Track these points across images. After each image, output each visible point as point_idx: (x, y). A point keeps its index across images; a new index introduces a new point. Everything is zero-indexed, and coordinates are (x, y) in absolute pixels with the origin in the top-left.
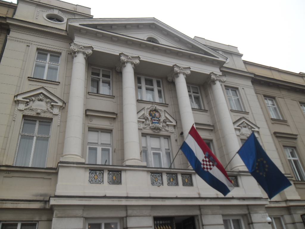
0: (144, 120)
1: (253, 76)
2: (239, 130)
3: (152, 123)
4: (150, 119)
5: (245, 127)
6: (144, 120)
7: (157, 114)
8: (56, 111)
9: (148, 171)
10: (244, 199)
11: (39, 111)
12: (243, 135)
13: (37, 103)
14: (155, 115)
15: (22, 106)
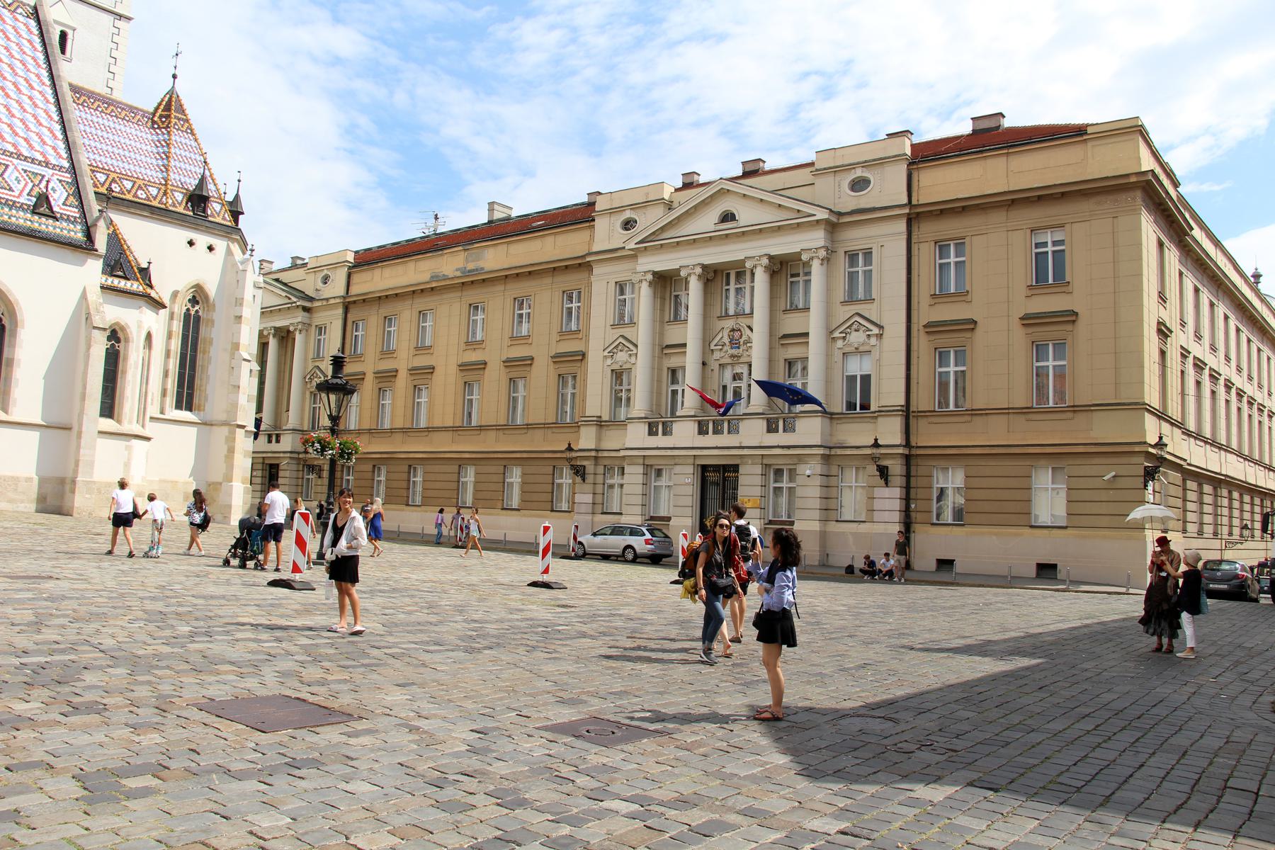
0: (720, 347)
1: (907, 211)
2: (844, 338)
3: (732, 348)
4: (728, 344)
5: (856, 330)
6: (720, 347)
7: (737, 334)
8: (633, 360)
9: (695, 420)
10: (789, 447)
11: (620, 364)
12: (850, 345)
13: (620, 353)
14: (733, 336)
15: (609, 361)
